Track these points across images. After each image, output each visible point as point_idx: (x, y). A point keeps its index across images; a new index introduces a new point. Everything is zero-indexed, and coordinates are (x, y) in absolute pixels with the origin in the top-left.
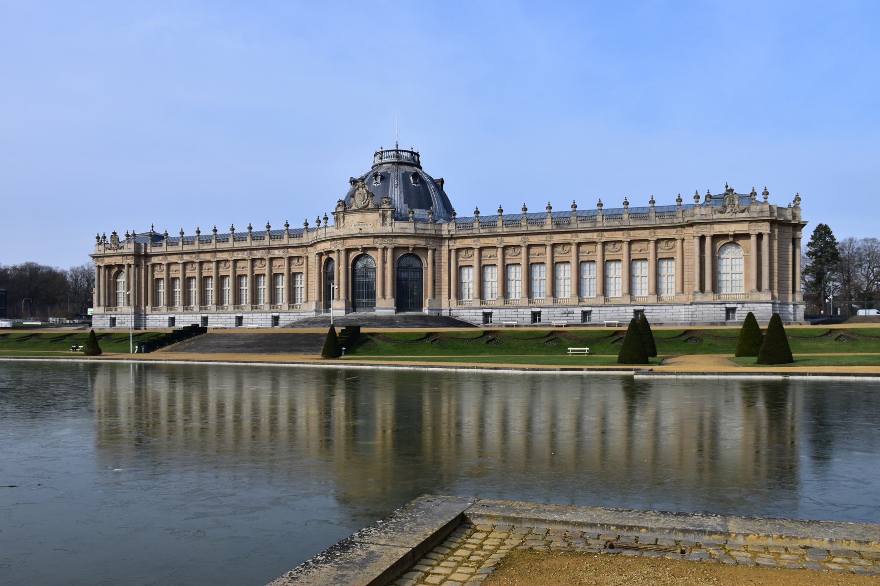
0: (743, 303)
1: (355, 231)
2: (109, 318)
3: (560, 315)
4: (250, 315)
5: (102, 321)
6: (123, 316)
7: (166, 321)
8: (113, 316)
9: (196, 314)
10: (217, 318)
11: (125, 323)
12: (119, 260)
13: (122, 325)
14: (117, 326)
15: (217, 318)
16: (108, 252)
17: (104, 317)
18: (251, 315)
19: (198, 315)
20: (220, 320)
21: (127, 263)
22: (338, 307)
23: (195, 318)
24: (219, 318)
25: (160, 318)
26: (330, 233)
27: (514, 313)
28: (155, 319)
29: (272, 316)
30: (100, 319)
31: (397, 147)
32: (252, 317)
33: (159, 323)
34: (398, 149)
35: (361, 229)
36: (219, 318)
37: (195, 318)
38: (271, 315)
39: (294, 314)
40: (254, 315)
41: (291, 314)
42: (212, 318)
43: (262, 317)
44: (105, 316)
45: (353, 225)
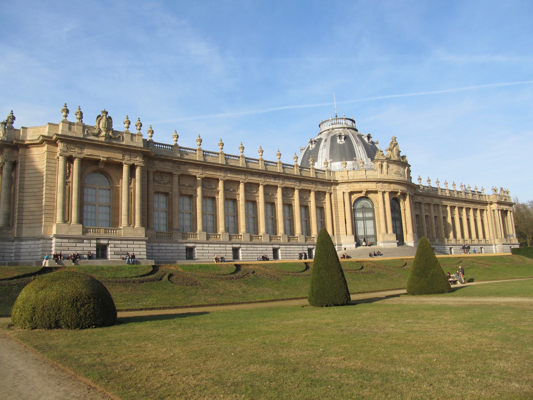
2: (95, 245)
7: (182, 251)
12: (117, 156)
15: (252, 249)
19: (228, 246)
20: (256, 252)
21: (131, 163)
22: (391, 239)
23: (224, 249)
25: (172, 248)
28: (163, 248)
29: (308, 248)
30: (74, 244)
33: (171, 254)
37: (224, 249)
45: (393, 173)
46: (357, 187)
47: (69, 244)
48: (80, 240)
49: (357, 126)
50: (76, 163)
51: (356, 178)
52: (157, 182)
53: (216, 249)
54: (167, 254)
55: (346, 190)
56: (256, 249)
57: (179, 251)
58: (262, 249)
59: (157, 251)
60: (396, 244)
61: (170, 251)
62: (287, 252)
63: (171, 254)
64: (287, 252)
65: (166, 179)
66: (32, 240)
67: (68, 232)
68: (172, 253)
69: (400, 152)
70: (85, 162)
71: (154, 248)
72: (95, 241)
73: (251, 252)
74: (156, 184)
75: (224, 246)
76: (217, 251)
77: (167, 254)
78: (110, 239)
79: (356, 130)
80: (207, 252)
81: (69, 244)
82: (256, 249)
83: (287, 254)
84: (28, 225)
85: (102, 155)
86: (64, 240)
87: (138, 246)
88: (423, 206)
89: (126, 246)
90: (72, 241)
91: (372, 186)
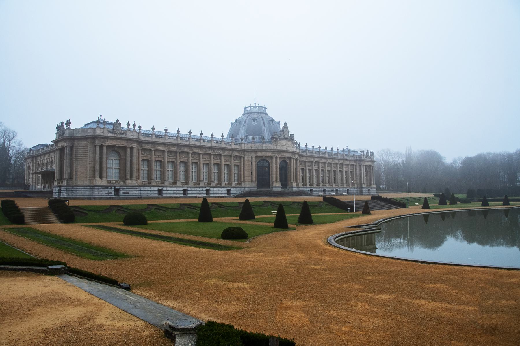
0: (371, 188)
1: (284, 149)
2: (114, 189)
3: (330, 191)
4: (214, 188)
5: (105, 191)
6: (128, 188)
8: (118, 188)
9: (179, 187)
10: (194, 190)
11: (130, 193)
13: (127, 195)
14: (122, 195)
15: (194, 190)
16: (110, 135)
17: (108, 188)
18: (215, 188)
19: (180, 188)
22: (277, 186)
24: (195, 190)
25: (150, 190)
26: (269, 147)
27: (319, 190)
28: (146, 190)
29: (227, 189)
30: (104, 189)
31: (255, 104)
32: (216, 190)
33: (150, 193)
34: (256, 106)
35: (287, 148)
36: (195, 190)
38: (226, 188)
39: (239, 189)
40: (217, 188)
41: (237, 189)
42: (190, 190)
43: (221, 190)
44: (109, 187)
46: (259, 154)
47: (102, 189)
48: (106, 187)
49: (268, 112)
50: (105, 149)
51: (259, 148)
52: (143, 154)
53: (174, 190)
54: (148, 193)
55: (253, 155)
56: (196, 190)
57: (154, 191)
58: (199, 190)
59: (143, 191)
60: (281, 188)
61: (150, 191)
62: (214, 191)
63: (150, 193)
64: (214, 191)
65: (147, 153)
66: (83, 186)
67: (101, 183)
68: (150, 192)
69: (289, 132)
70: (108, 147)
71: (141, 190)
72: (114, 188)
73: (193, 191)
74: (142, 155)
75: (178, 188)
76: (174, 191)
77: (148, 193)
78: (121, 186)
79: (267, 114)
80: (169, 191)
81: (102, 189)
82: (196, 190)
83: (214, 193)
84: (80, 179)
85: (117, 143)
86: (99, 187)
87: (134, 189)
88: (307, 163)
89: (128, 189)
90: (103, 187)
91: (269, 154)
